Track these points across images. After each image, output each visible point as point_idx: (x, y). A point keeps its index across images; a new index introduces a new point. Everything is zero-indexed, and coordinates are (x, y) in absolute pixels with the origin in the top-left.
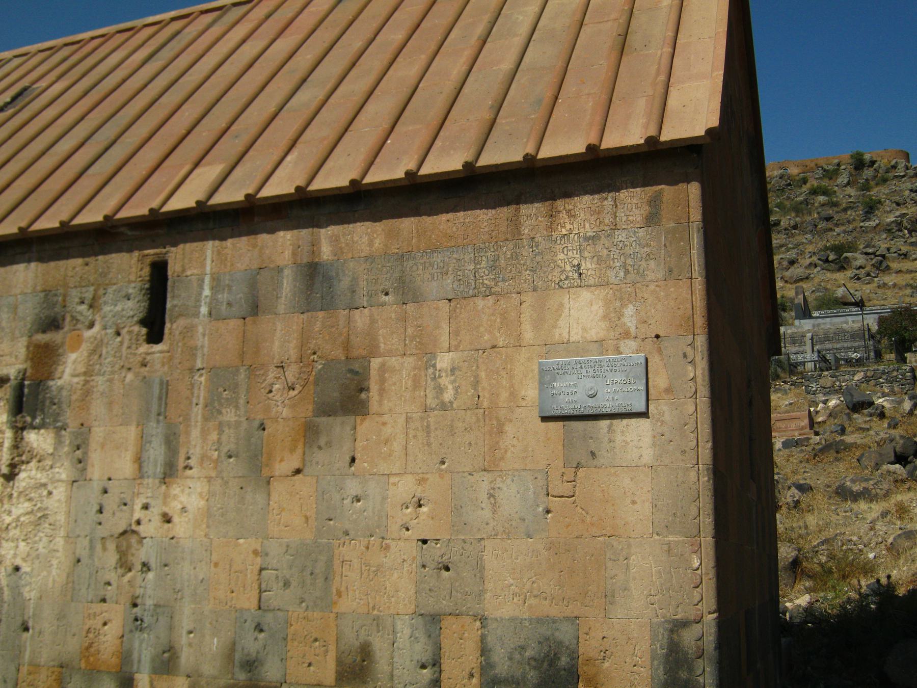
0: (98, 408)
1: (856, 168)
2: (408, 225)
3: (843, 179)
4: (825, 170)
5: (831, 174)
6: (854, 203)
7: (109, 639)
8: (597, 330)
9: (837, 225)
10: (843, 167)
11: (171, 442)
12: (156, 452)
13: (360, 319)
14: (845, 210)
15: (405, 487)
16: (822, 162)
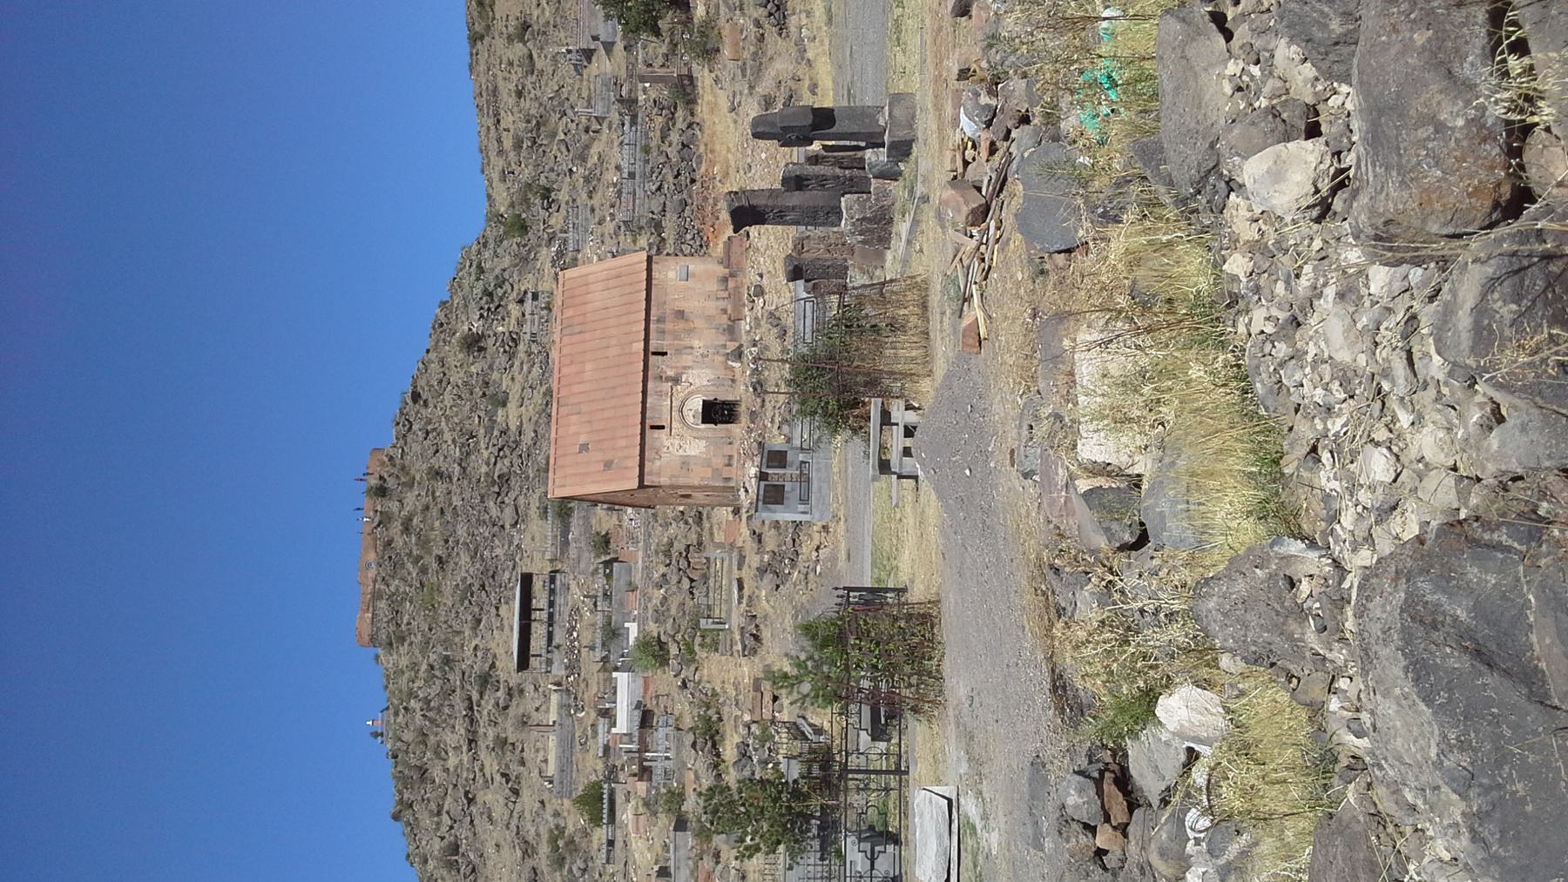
0: (678, 365)
1: (384, 496)
2: (652, 303)
3: (394, 506)
4: (379, 525)
5: (385, 520)
6: (428, 490)
7: (721, 359)
8: (674, 272)
9: (450, 504)
10: (379, 508)
11: (686, 348)
12: (689, 351)
13: (668, 311)
14: (434, 498)
15: (696, 303)
16: (368, 529)
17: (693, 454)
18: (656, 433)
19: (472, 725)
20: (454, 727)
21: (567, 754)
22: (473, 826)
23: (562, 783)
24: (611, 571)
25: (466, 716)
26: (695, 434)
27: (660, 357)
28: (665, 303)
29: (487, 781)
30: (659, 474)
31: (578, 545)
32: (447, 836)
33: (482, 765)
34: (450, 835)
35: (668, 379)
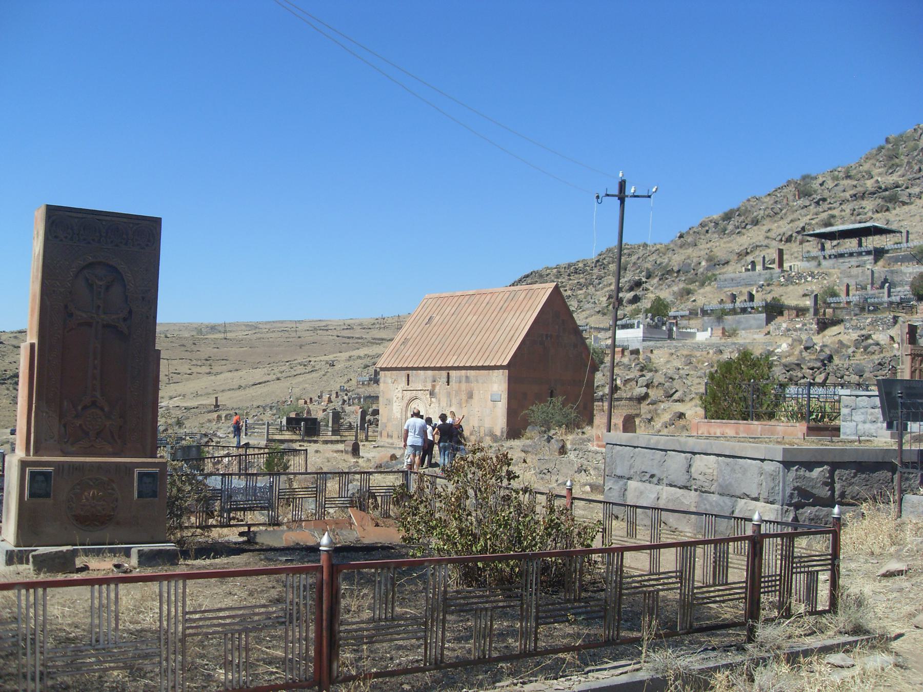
11: (451, 401)
12: (449, 403)
15: (477, 409)
17: (394, 408)
18: (404, 379)
19: (869, 194)
20: (903, 176)
21: (742, 282)
22: (802, 208)
23: (726, 280)
24: (761, 312)
25: (880, 188)
26: (404, 409)
27: (446, 380)
28: (477, 381)
29: (817, 214)
30: (384, 382)
31: (860, 275)
32: (823, 188)
33: (834, 209)
34: (823, 190)
35: (434, 386)
